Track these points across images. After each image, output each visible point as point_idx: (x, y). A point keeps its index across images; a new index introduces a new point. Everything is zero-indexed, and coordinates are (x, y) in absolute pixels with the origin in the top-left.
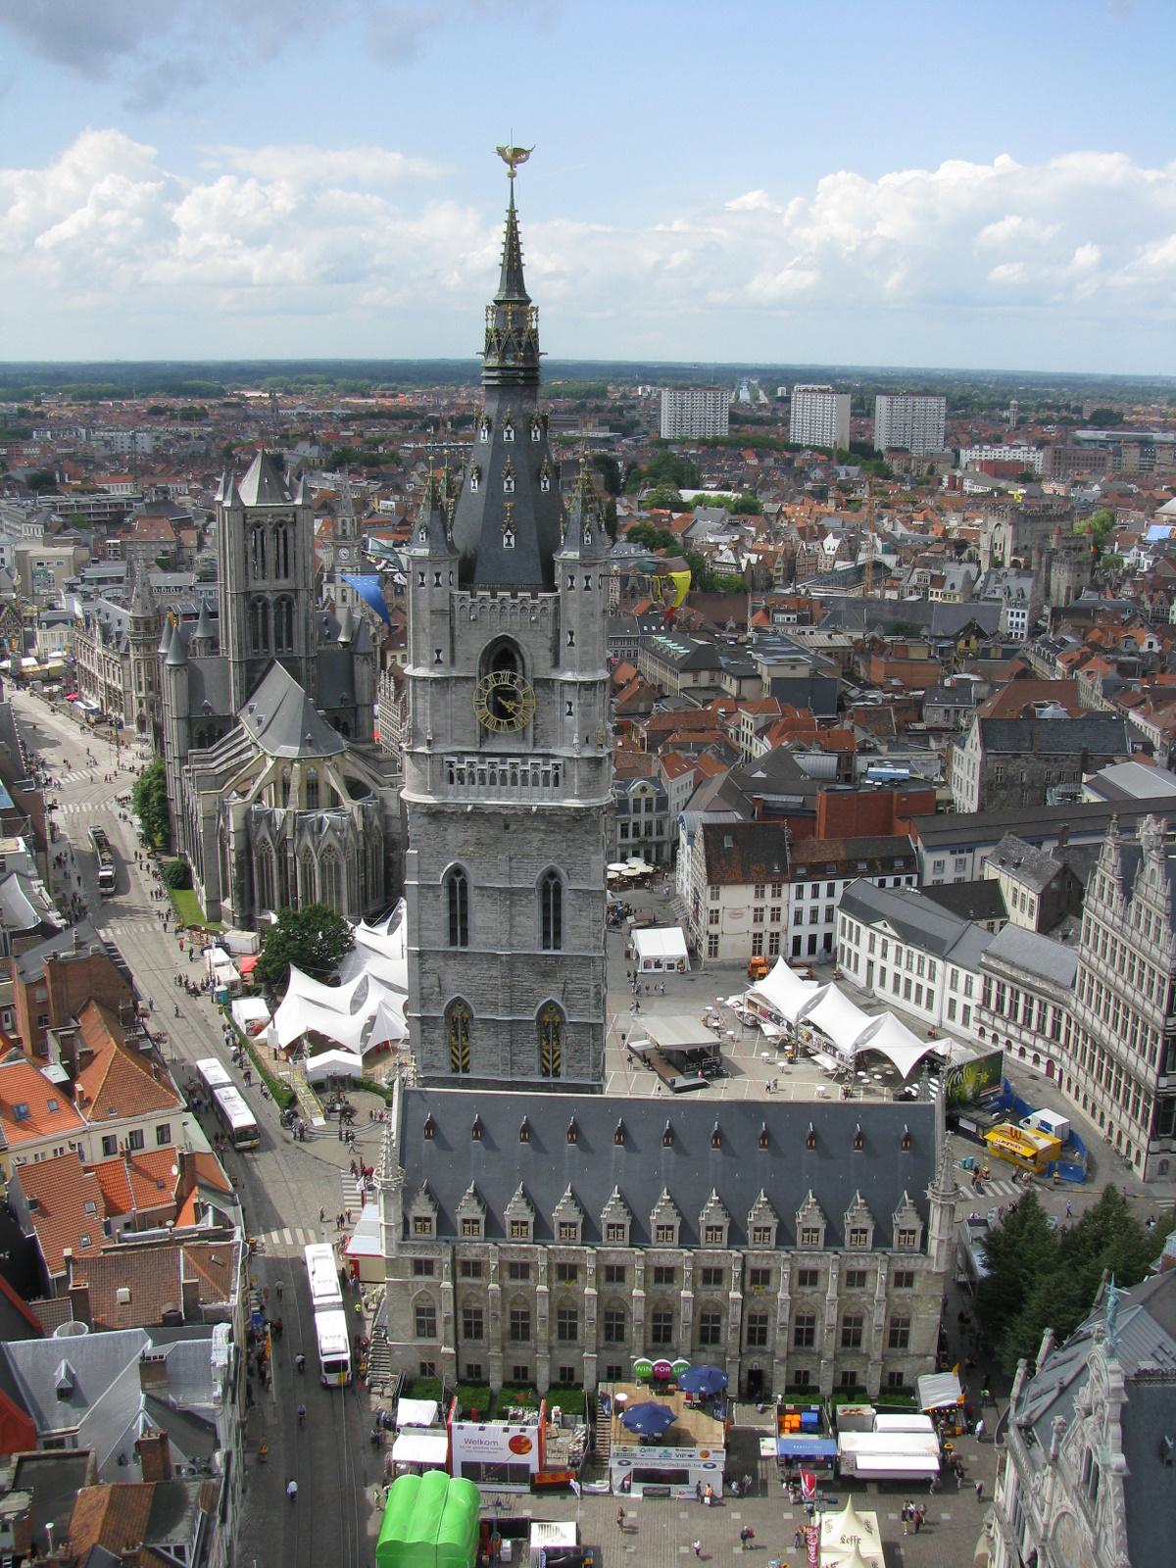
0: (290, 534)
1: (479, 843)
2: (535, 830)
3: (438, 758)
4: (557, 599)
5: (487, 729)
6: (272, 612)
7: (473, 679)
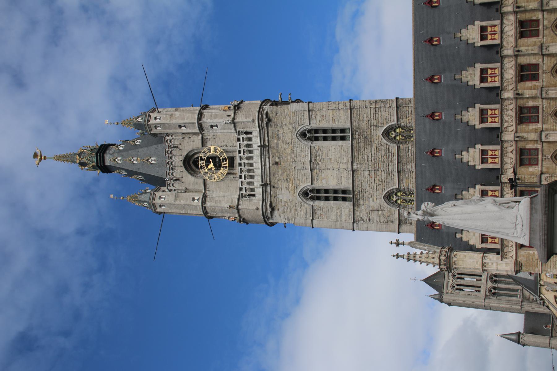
0: (459, 271)
1: (287, 179)
2: (277, 144)
4: (168, 135)
5: (228, 174)
6: (497, 285)
7: (204, 180)
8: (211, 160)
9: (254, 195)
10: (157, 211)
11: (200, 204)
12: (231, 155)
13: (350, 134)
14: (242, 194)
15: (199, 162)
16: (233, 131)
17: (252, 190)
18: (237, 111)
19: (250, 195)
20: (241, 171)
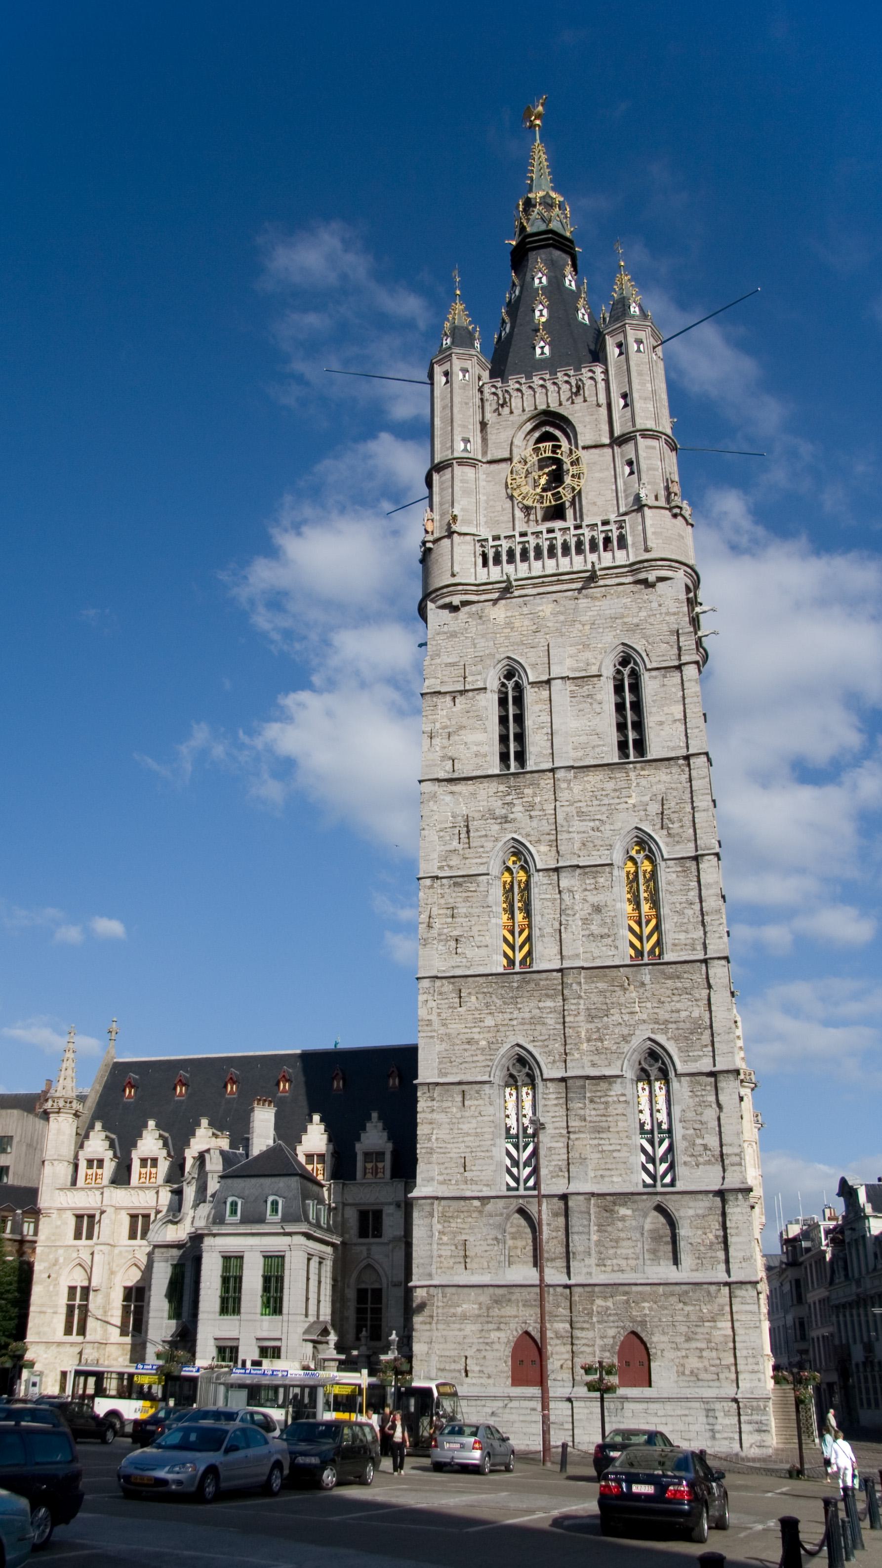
3: (468, 537)
8: (554, 467)
9: (485, 564)
10: (435, 366)
11: (456, 455)
12: (569, 513)
13: (632, 759)
14: (486, 540)
15: (547, 444)
16: (623, 509)
17: (497, 561)
18: (667, 512)
19: (484, 556)
20: (537, 534)
